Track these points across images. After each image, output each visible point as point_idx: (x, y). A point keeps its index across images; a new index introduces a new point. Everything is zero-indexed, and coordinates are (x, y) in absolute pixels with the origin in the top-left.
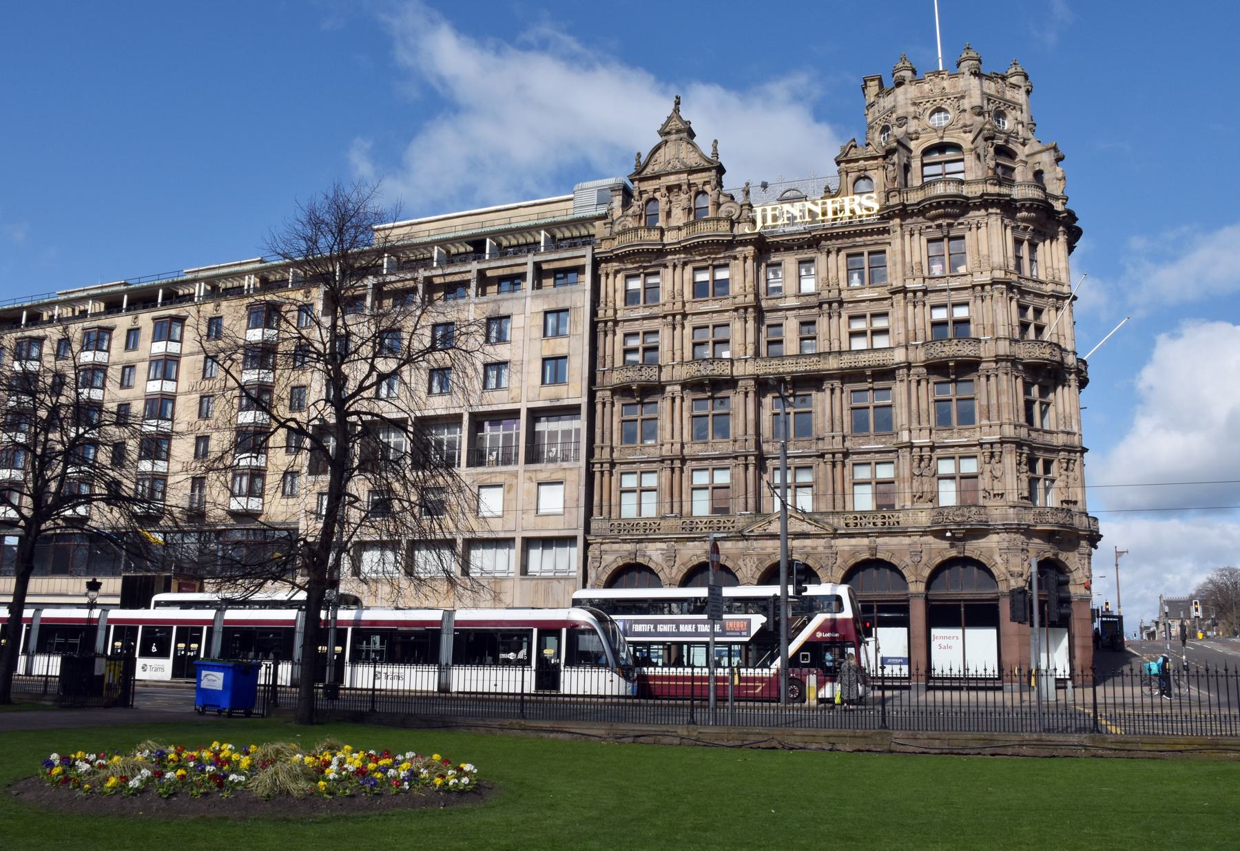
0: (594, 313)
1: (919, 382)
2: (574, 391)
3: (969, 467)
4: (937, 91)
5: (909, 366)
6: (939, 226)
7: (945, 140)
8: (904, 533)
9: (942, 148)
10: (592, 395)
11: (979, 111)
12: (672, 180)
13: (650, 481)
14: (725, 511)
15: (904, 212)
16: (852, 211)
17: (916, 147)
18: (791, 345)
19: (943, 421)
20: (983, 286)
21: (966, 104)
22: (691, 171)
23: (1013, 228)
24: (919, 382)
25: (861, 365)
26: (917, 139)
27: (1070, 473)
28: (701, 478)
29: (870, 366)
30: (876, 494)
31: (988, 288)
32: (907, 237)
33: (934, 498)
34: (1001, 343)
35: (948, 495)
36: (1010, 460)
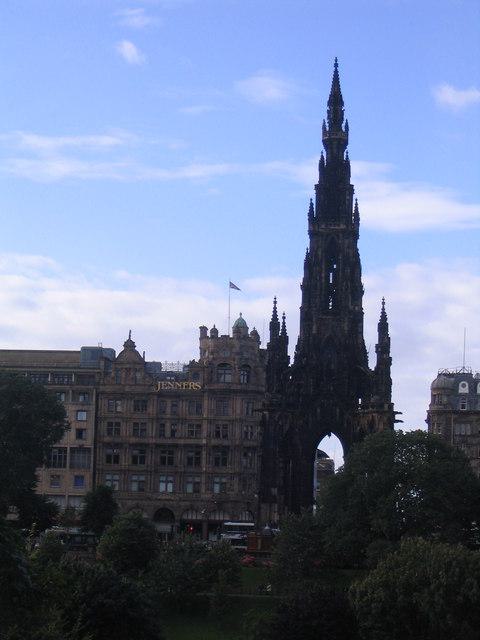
0: (96, 413)
2: (88, 442)
3: (224, 480)
8: (202, 501)
9: (224, 365)
10: (95, 444)
11: (238, 354)
12: (128, 366)
13: (117, 477)
14: (143, 490)
15: (212, 392)
17: (216, 363)
18: (168, 433)
19: (217, 464)
22: (135, 363)
28: (135, 478)
30: (194, 487)
33: (212, 490)
35: (217, 488)
36: (236, 480)
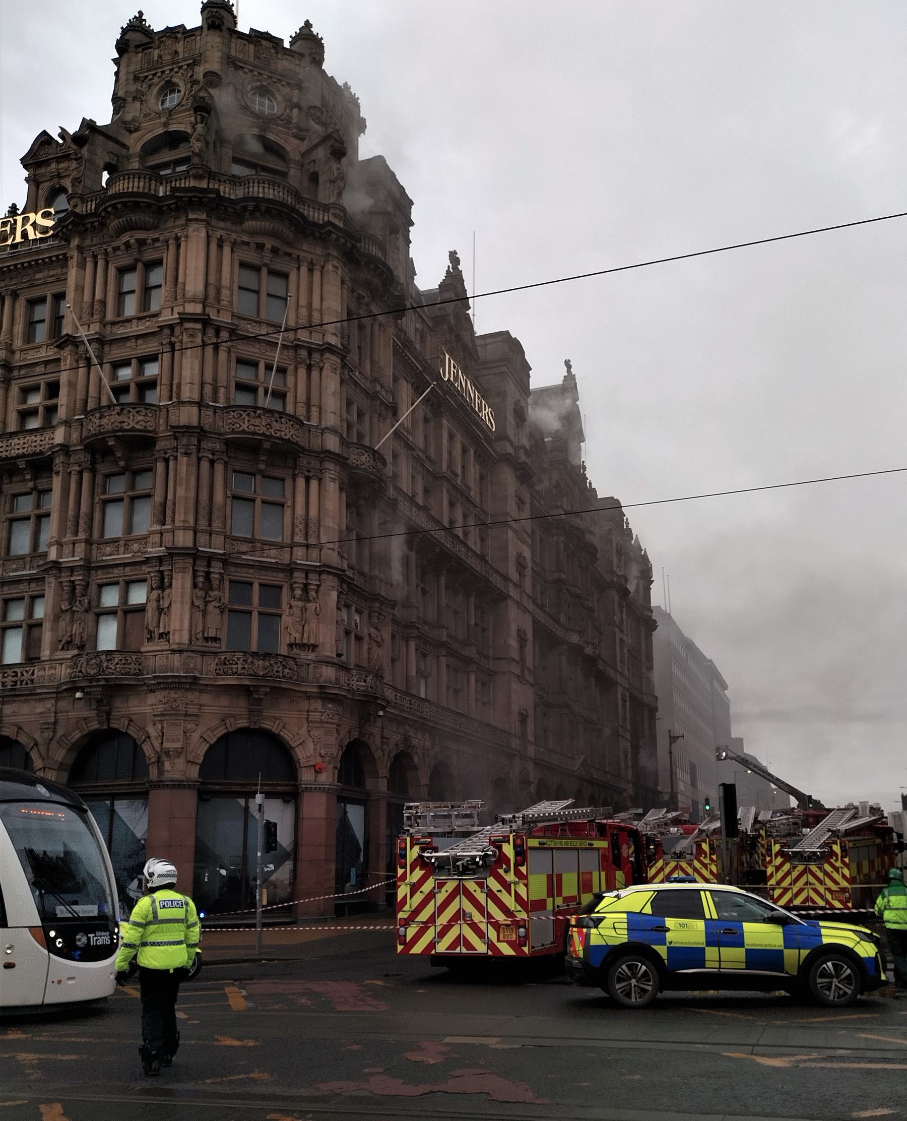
1: (80, 473)
4: (167, 58)
5: (65, 448)
6: (127, 245)
7: (172, 128)
16: (24, 234)
20: (171, 327)
21: (200, 71)
23: (234, 244)
24: (80, 473)
25: (14, 453)
26: (137, 130)
27: (311, 606)
29: (24, 456)
31: (177, 330)
32: (89, 266)
34: (185, 410)
